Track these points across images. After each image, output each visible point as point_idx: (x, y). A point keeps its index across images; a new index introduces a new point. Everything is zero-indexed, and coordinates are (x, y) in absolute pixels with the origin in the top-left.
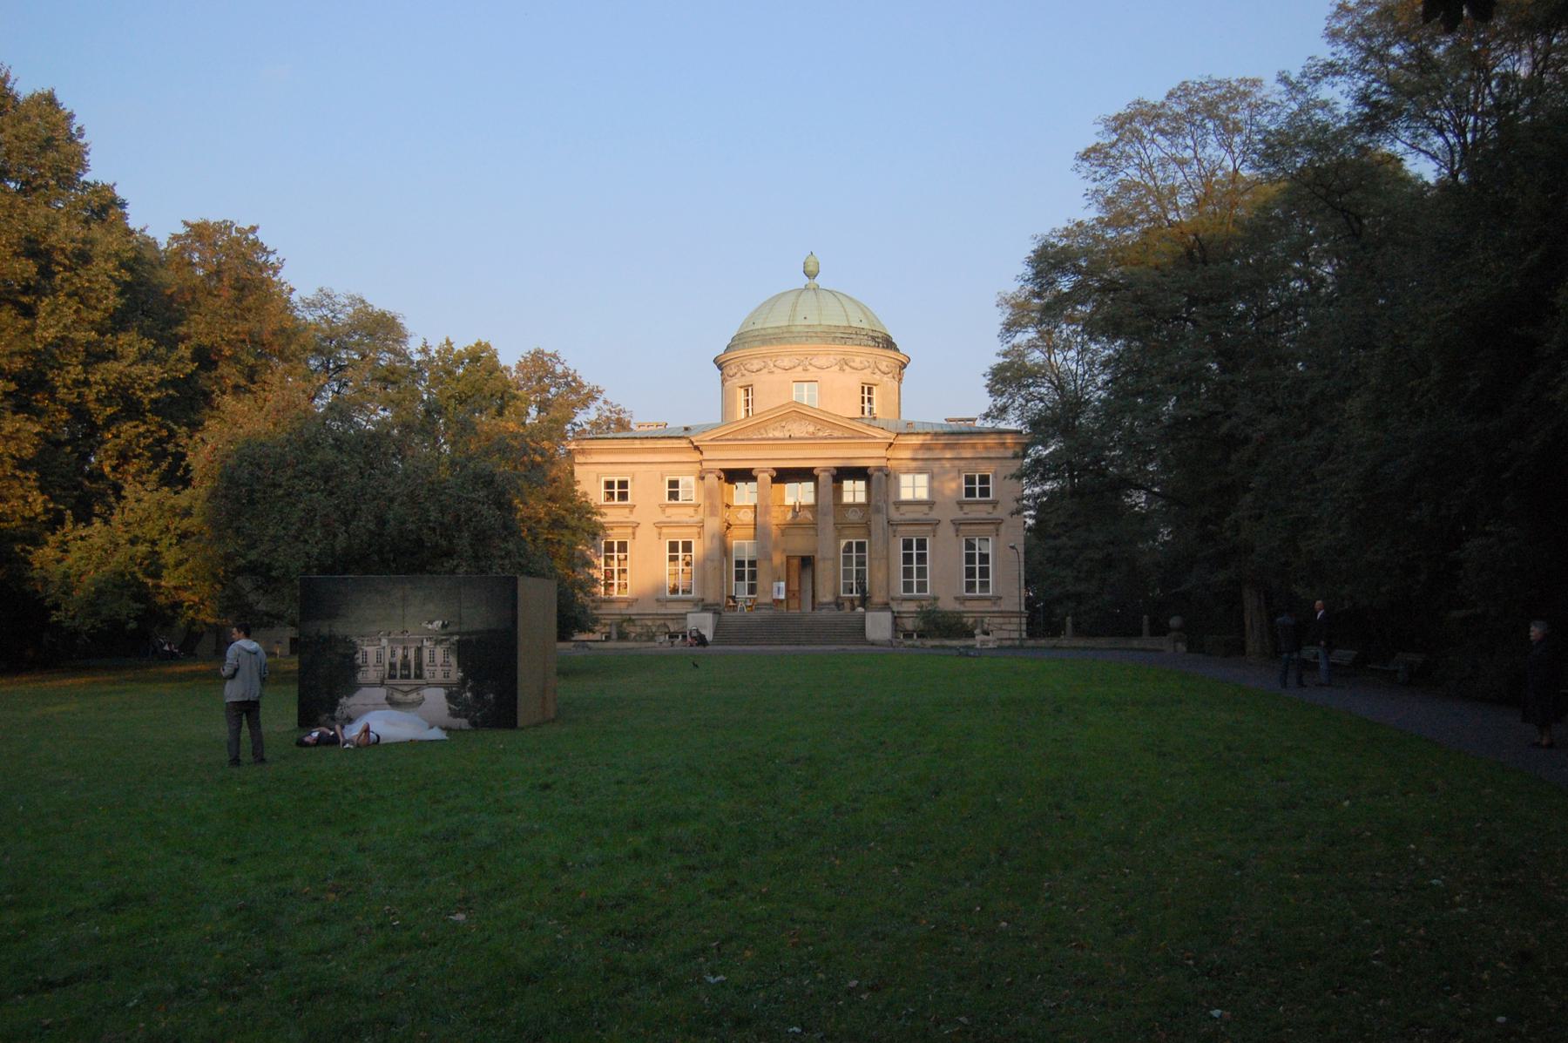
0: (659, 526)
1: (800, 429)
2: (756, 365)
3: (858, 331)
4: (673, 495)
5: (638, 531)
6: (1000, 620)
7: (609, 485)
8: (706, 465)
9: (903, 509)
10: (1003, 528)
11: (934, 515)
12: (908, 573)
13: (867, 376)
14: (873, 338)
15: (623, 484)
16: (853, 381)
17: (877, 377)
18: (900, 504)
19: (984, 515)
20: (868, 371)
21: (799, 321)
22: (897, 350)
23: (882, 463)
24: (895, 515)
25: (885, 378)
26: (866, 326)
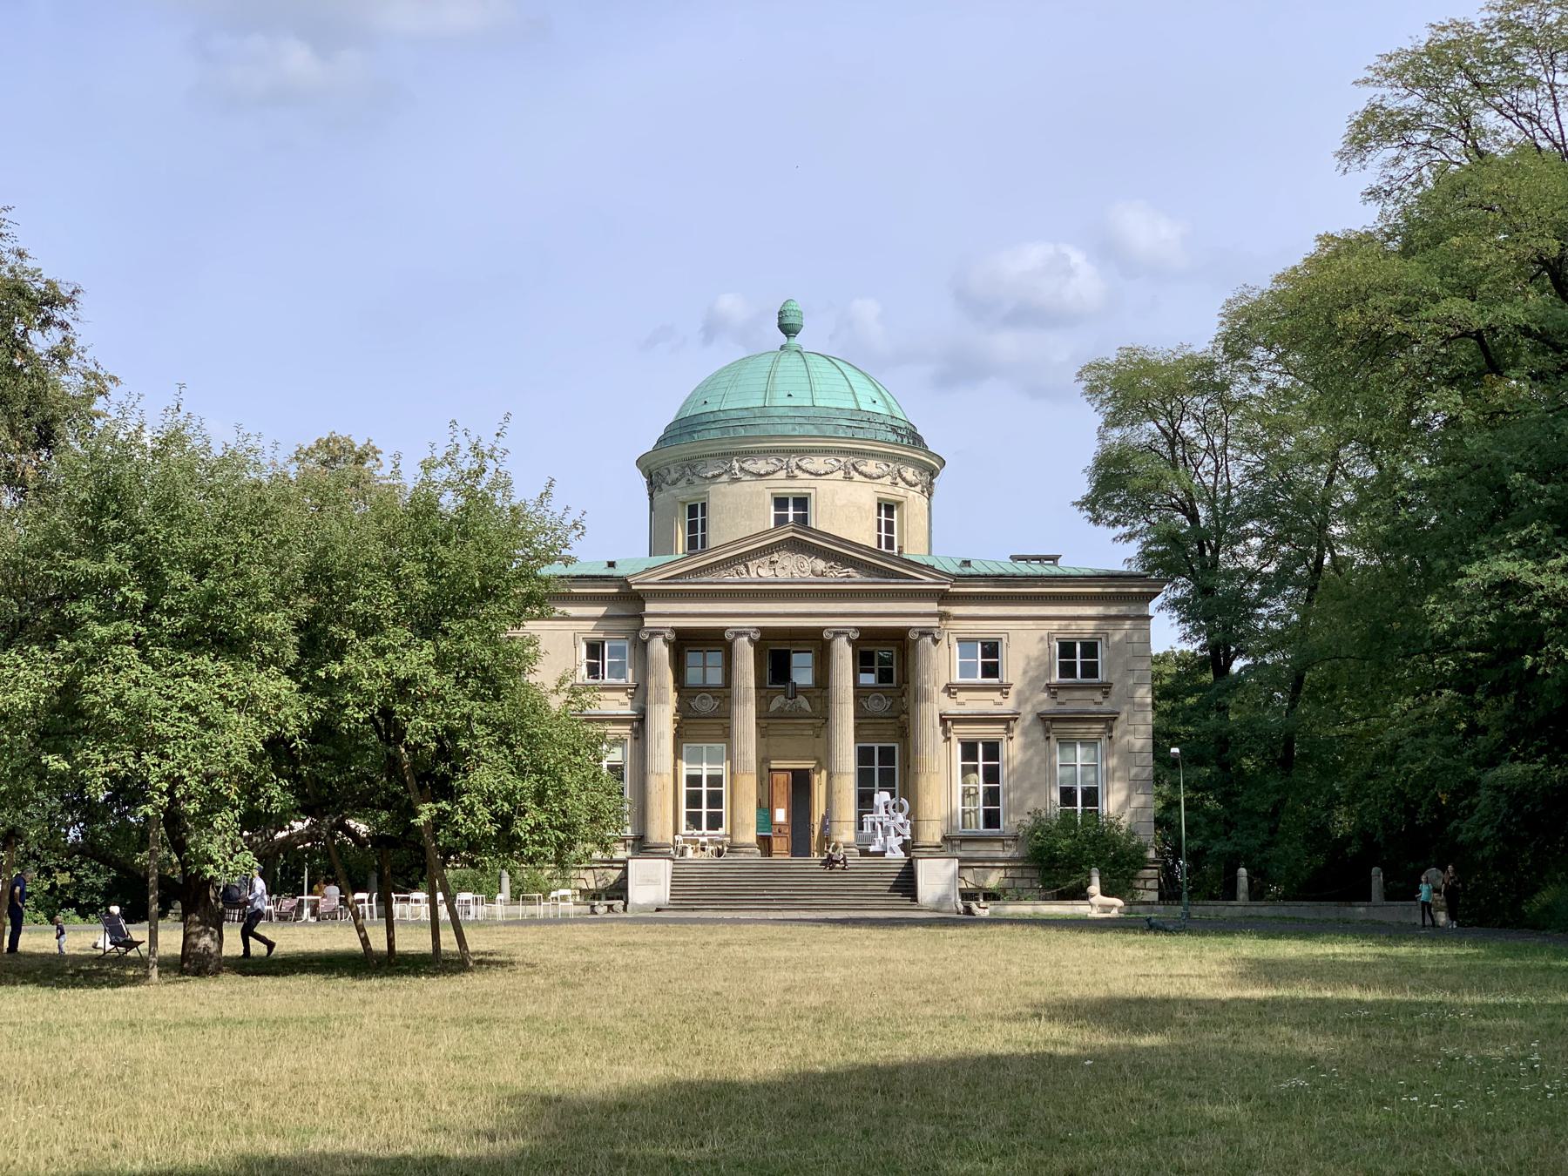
9: (962, 696)
14: (894, 430)
16: (864, 496)
17: (901, 490)
19: (1094, 708)
20: (887, 480)
21: (780, 400)
26: (884, 411)
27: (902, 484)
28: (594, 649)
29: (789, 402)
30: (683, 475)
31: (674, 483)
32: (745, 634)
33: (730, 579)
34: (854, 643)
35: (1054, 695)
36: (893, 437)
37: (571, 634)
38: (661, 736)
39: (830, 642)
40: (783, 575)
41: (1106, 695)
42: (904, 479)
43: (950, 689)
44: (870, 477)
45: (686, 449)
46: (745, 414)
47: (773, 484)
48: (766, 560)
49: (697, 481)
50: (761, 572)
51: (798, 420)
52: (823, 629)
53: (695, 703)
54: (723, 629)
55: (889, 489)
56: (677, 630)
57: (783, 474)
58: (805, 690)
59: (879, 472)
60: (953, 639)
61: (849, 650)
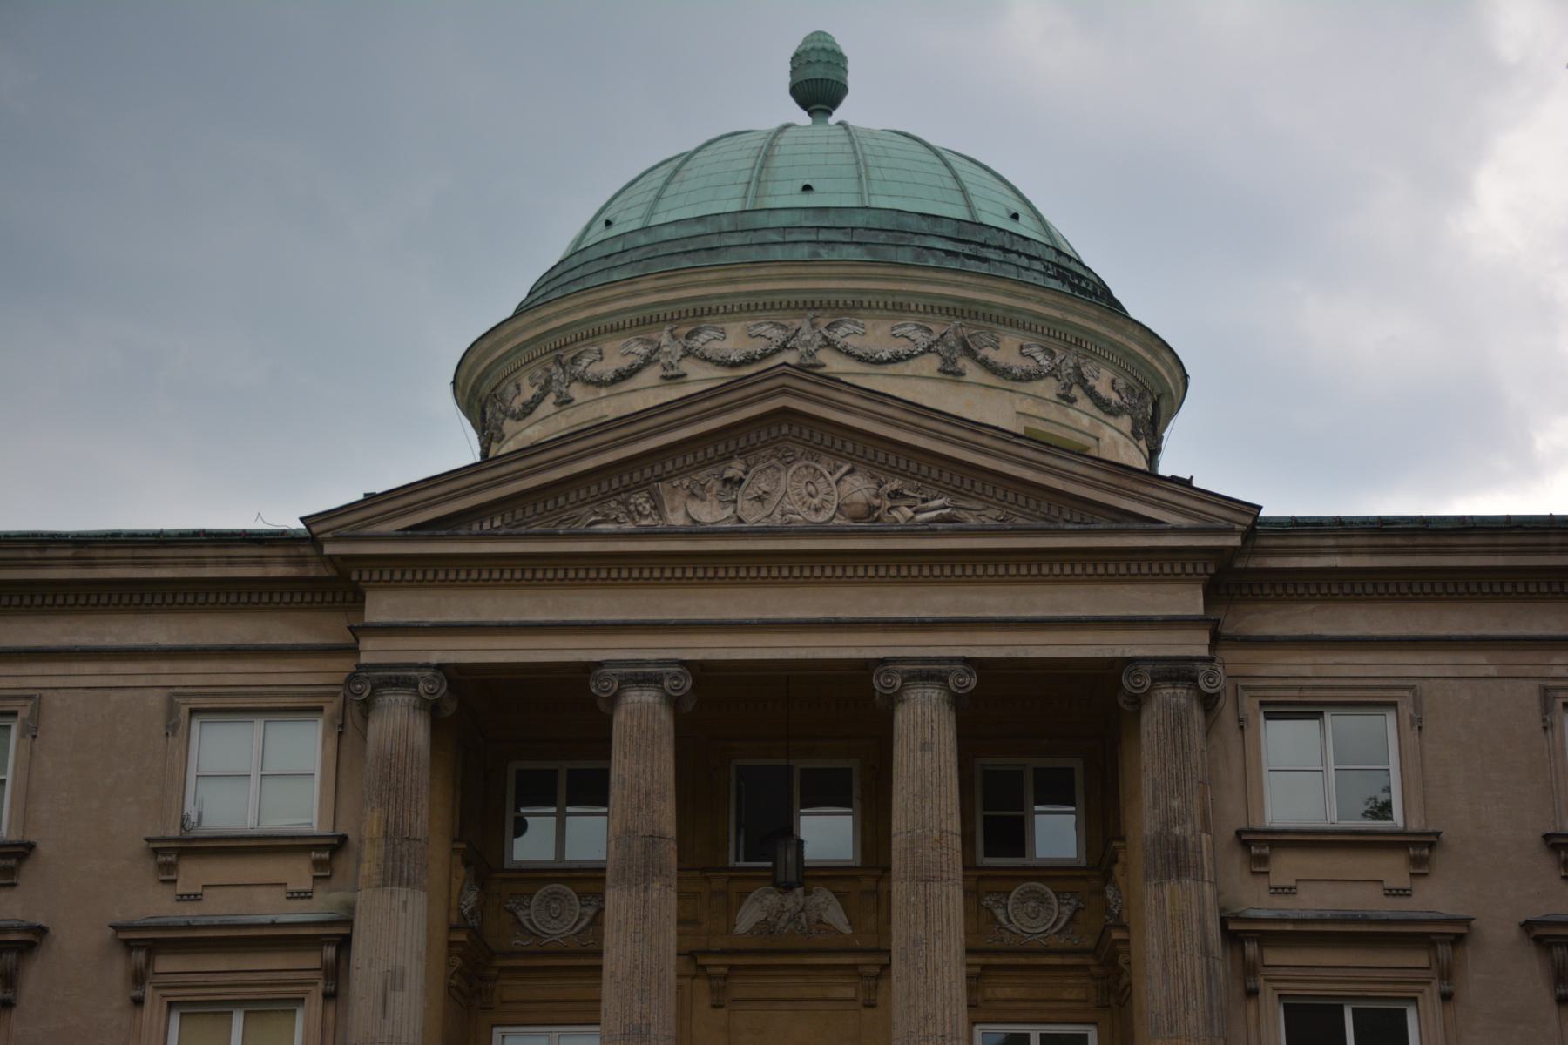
1: (804, 496)
8: (374, 651)
9: (1286, 867)
11: (1436, 898)
18: (1259, 845)
23: (1194, 645)
24: (1256, 900)
27: (1084, 403)
30: (545, 390)
31: (529, 408)
33: (609, 530)
37: (156, 700)
38: (394, 980)
39: (893, 700)
40: (754, 516)
42: (1091, 393)
45: (559, 317)
46: (699, 229)
49: (577, 392)
51: (824, 236)
53: (533, 913)
54: (588, 669)
55: (1053, 413)
56: (452, 673)
58: (831, 875)
60: (1250, 704)
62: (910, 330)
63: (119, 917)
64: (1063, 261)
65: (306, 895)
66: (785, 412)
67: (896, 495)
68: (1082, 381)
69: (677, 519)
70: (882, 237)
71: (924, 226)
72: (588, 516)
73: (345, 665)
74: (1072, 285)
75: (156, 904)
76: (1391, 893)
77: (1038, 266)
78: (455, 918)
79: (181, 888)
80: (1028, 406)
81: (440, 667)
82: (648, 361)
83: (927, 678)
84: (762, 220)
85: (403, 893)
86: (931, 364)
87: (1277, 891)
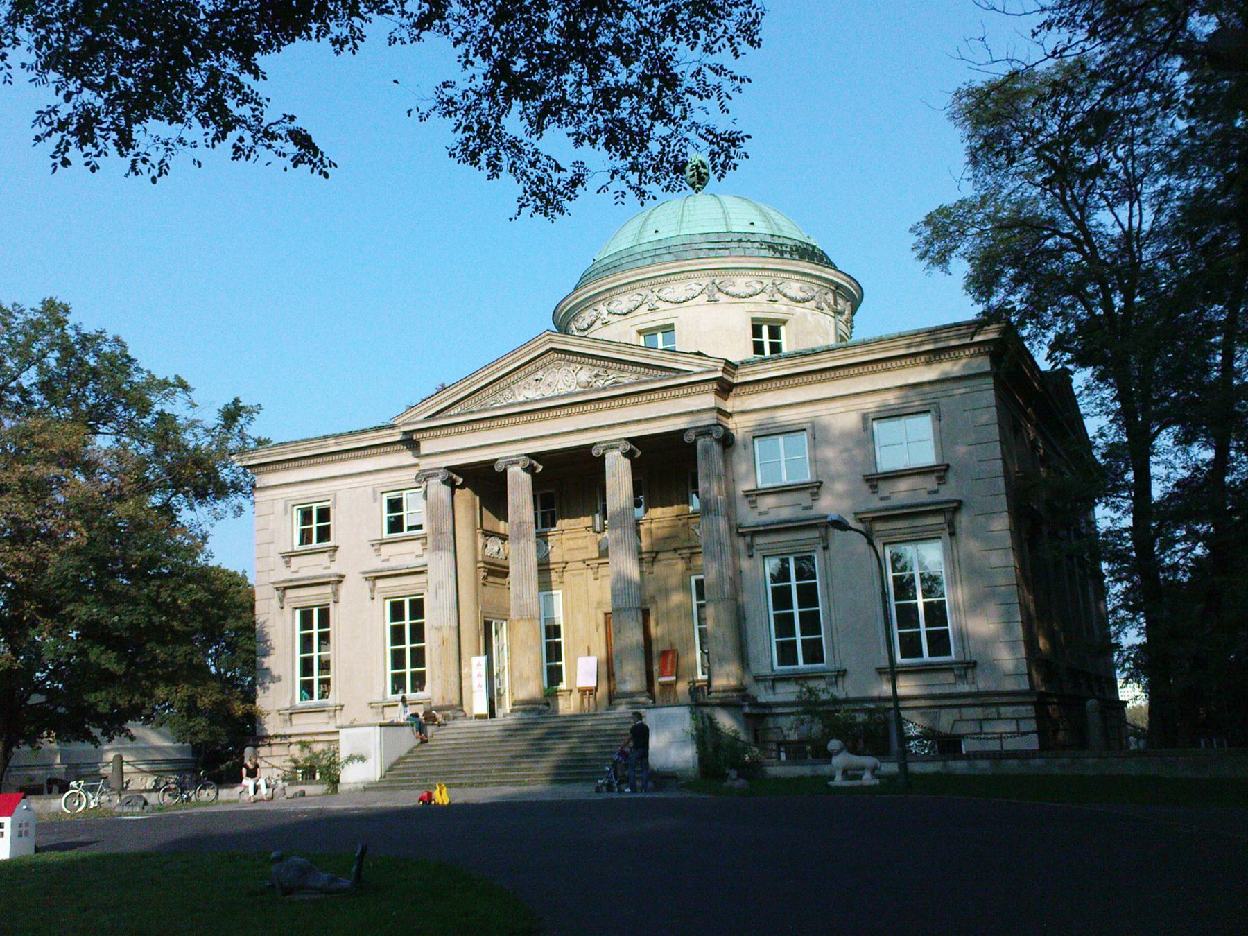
0: (374, 578)
2: (587, 317)
3: (743, 240)
4: (396, 525)
5: (343, 589)
6: (977, 713)
7: (306, 516)
8: (426, 464)
10: (963, 520)
12: (784, 625)
13: (763, 308)
15: (324, 514)
17: (781, 309)
20: (763, 298)
22: (830, 264)
24: (749, 517)
25: (799, 310)
28: (395, 505)
29: (658, 237)
32: (516, 463)
34: (628, 455)
35: (874, 488)
36: (772, 253)
37: (370, 490)
38: (440, 585)
40: (548, 394)
41: (942, 480)
42: (785, 295)
43: (755, 495)
44: (738, 296)
47: (636, 320)
48: (531, 379)
50: (526, 393)
52: (592, 445)
57: (644, 308)
59: (750, 291)
61: (626, 463)
62: (693, 286)
63: (365, 569)
64: (777, 240)
65: (421, 556)
66: (552, 349)
67: (596, 376)
68: (780, 292)
69: (521, 399)
70: (681, 248)
71: (703, 239)
72: (490, 401)
73: (415, 471)
74: (775, 250)
75: (376, 564)
76: (805, 508)
77: (757, 245)
78: (480, 558)
79: (382, 557)
80: (752, 308)
81: (446, 468)
82: (598, 318)
83: (612, 448)
84: (638, 249)
85: (440, 553)
86: (704, 297)
87: (760, 514)
